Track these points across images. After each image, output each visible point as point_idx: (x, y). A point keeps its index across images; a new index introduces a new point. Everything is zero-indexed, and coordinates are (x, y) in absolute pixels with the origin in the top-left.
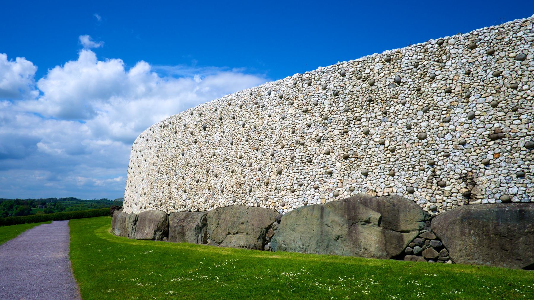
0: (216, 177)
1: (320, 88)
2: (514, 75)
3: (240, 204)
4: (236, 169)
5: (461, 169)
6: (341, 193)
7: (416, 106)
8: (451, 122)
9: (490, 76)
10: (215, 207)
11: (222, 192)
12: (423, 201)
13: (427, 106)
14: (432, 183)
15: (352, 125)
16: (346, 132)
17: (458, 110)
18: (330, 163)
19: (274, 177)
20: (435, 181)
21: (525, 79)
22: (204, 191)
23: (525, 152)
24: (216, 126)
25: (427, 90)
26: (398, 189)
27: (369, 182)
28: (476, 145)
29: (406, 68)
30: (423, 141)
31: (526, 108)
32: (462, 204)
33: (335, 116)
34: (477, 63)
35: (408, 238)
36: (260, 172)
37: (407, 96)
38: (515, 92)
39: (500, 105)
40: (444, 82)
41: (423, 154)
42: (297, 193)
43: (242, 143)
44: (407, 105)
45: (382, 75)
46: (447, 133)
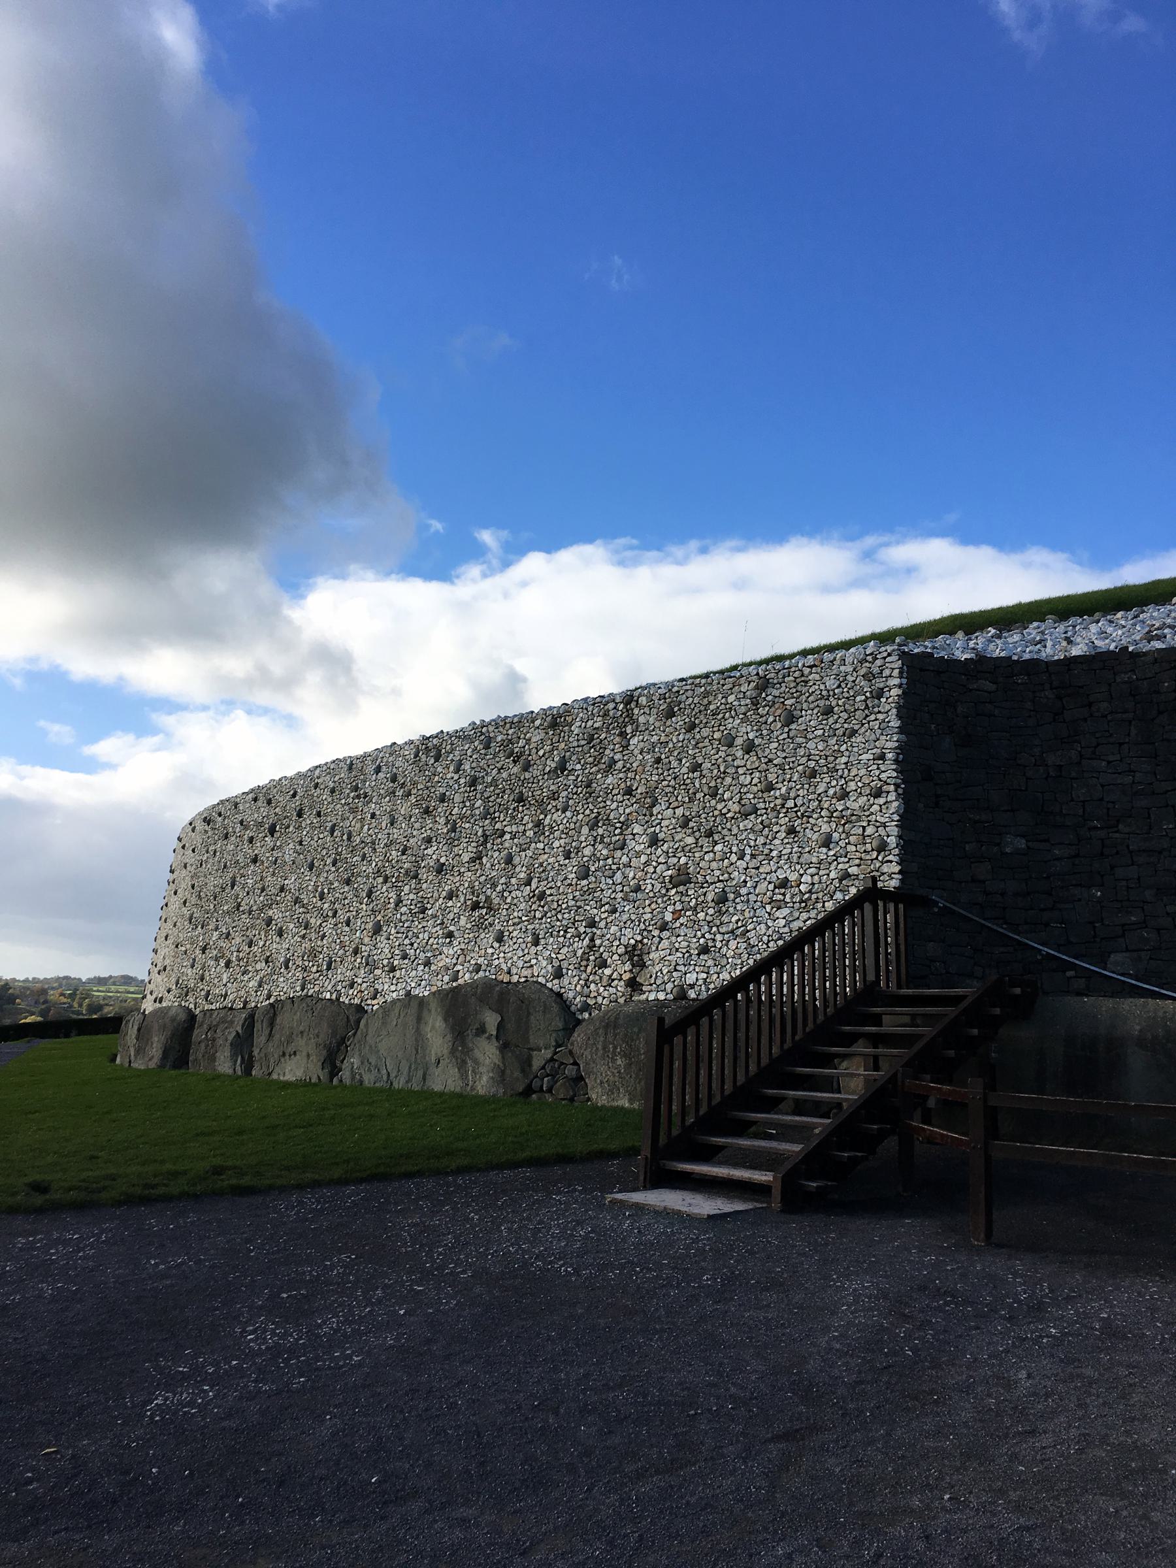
0: (280, 935)
1: (452, 768)
2: (715, 771)
3: (311, 992)
4: (313, 921)
5: (630, 936)
6: (461, 974)
7: (580, 817)
8: (626, 851)
9: (684, 770)
10: (272, 1000)
11: (287, 967)
12: (571, 995)
13: (596, 817)
14: (588, 960)
15: (489, 845)
16: (480, 858)
17: (637, 829)
18: (451, 916)
19: (367, 940)
20: (592, 958)
21: (728, 780)
22: (258, 966)
23: (711, 911)
24: (291, 829)
25: (598, 789)
26: (542, 970)
27: (502, 955)
28: (651, 894)
29: (575, 744)
30: (585, 882)
31: (725, 832)
32: (621, 1000)
33: (467, 825)
34: (671, 745)
35: (539, 1060)
36: (347, 929)
37: (570, 796)
38: (713, 802)
39: (691, 824)
40: (621, 775)
41: (580, 907)
42: (398, 974)
43: (327, 868)
44: (568, 814)
45: (541, 753)
46: (618, 869)
